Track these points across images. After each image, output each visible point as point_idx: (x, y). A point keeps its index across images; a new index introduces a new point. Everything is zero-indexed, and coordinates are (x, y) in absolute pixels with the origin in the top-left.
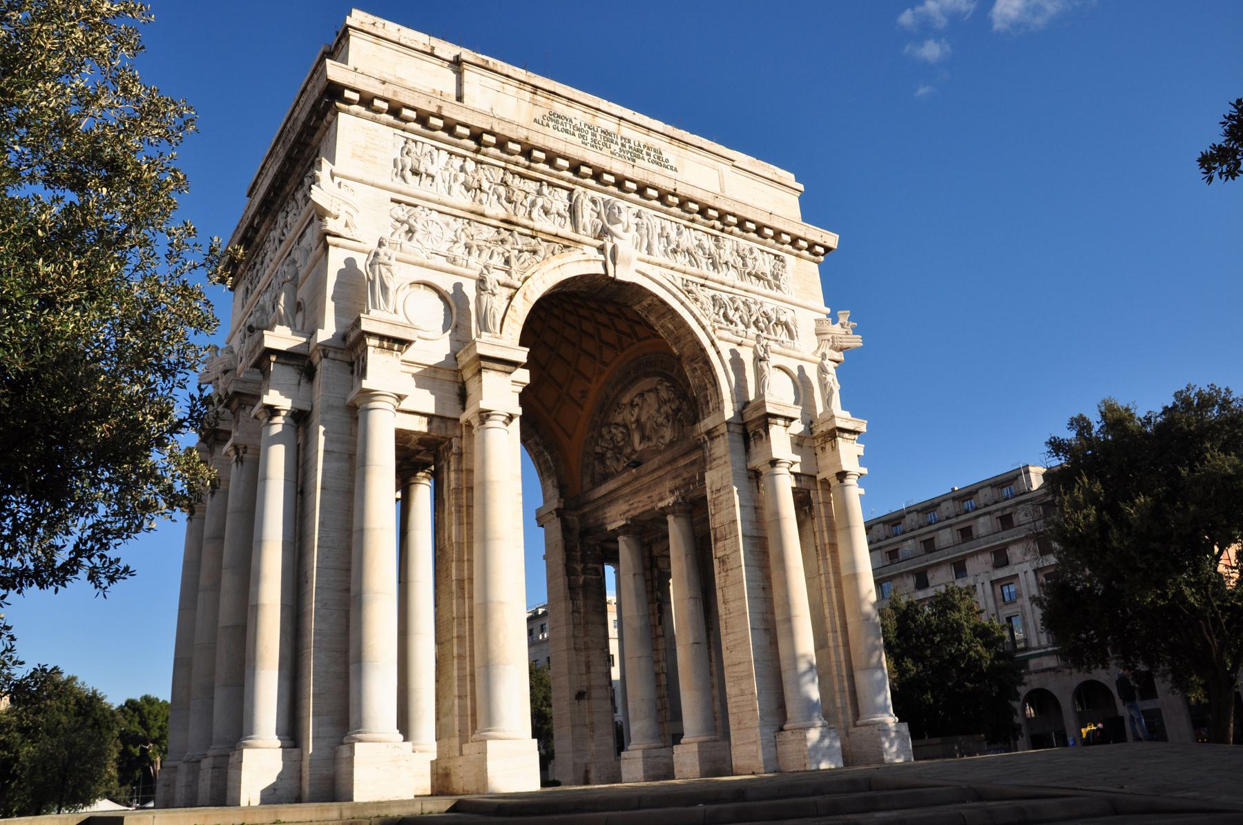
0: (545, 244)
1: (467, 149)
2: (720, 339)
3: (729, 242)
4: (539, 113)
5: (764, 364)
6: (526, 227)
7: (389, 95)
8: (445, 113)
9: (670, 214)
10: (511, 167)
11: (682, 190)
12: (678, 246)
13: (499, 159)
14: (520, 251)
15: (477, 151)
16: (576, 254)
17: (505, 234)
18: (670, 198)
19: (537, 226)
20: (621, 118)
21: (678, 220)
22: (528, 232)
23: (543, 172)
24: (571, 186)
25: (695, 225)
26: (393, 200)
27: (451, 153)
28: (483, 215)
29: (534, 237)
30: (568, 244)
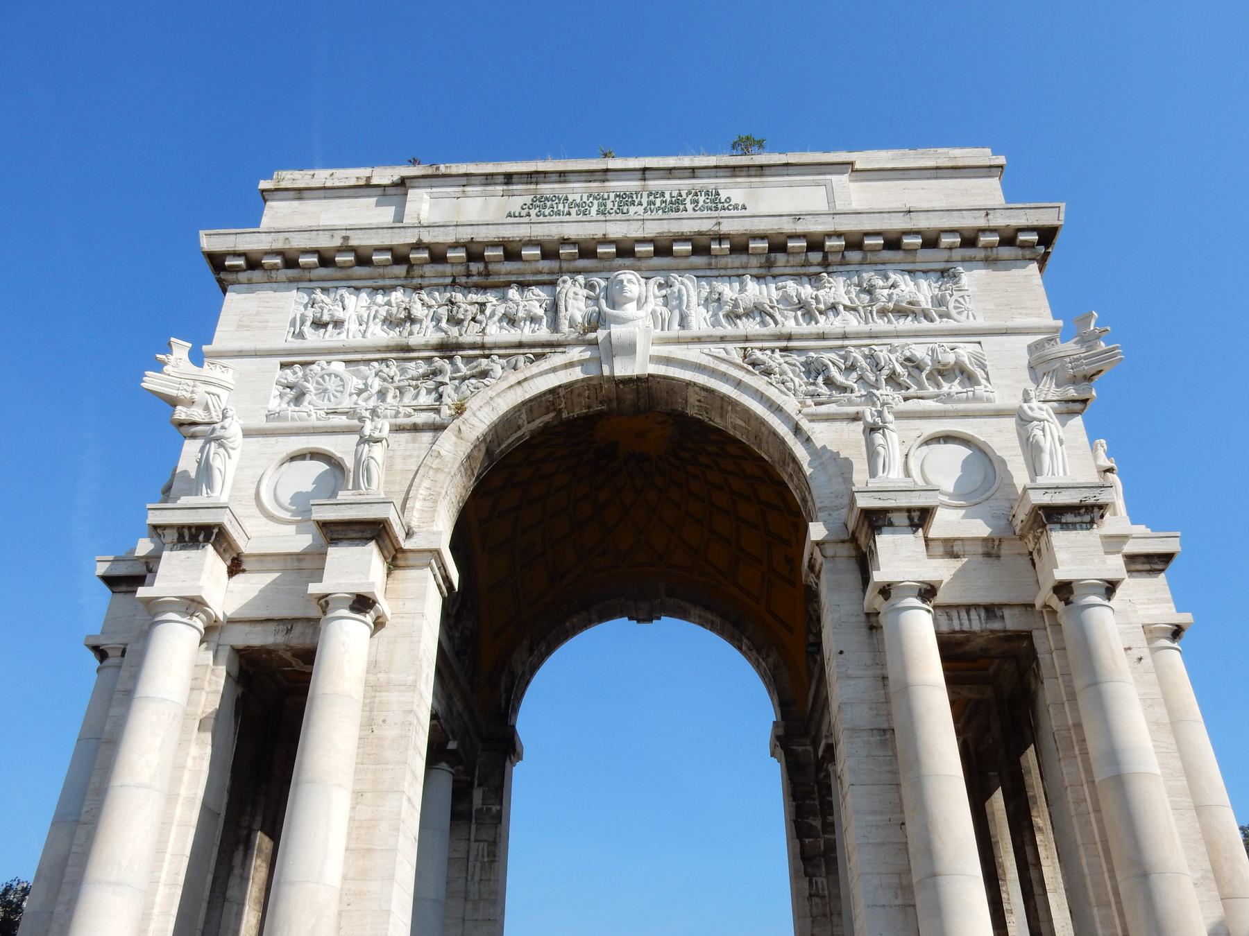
0: (503, 361)
1: (397, 278)
2: (814, 418)
4: (515, 204)
5: (878, 437)
8: (352, 242)
9: (726, 269)
12: (736, 305)
13: (444, 276)
14: (464, 379)
17: (438, 363)
18: (715, 246)
19: (488, 340)
23: (509, 273)
24: (555, 277)
25: (775, 271)
26: (283, 366)
28: (408, 349)
29: (488, 357)
30: (540, 350)
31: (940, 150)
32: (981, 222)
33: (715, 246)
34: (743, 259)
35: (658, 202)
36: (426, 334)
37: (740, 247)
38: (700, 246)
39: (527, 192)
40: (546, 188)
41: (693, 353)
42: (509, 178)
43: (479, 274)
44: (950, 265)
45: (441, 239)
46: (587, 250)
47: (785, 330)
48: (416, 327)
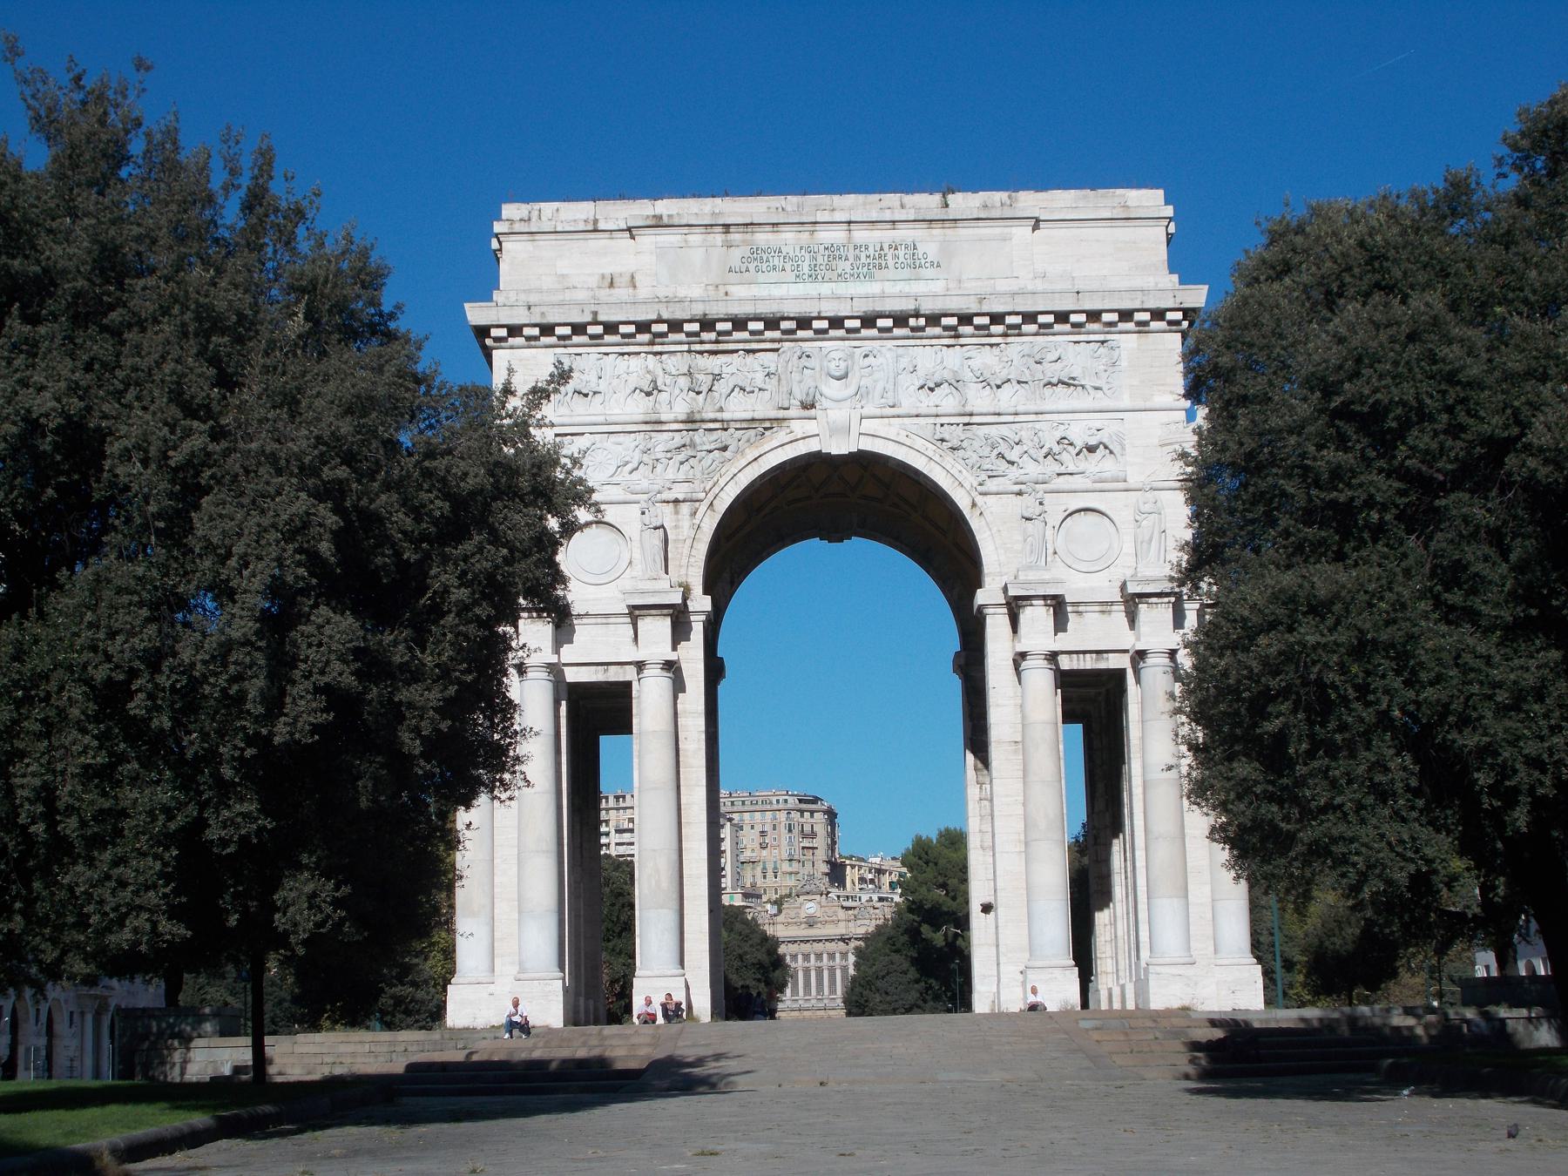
3: (1017, 346)
4: (736, 255)
6: (715, 421)
7: (538, 320)
8: (601, 318)
10: (698, 347)
11: (928, 307)
13: (680, 343)
15: (652, 343)
16: (781, 436)
18: (912, 322)
19: (726, 416)
20: (849, 222)
21: (934, 342)
22: (717, 425)
24: (776, 346)
25: (962, 341)
27: (623, 354)
31: (1119, 191)
32: (1138, 306)
33: (912, 322)
34: (937, 331)
35: (863, 256)
36: (676, 405)
37: (933, 320)
38: (900, 320)
39: (745, 242)
40: (762, 238)
41: (892, 428)
42: (727, 226)
43: (711, 342)
44: (1109, 337)
45: (679, 315)
46: (804, 323)
47: (968, 409)
48: (663, 397)
